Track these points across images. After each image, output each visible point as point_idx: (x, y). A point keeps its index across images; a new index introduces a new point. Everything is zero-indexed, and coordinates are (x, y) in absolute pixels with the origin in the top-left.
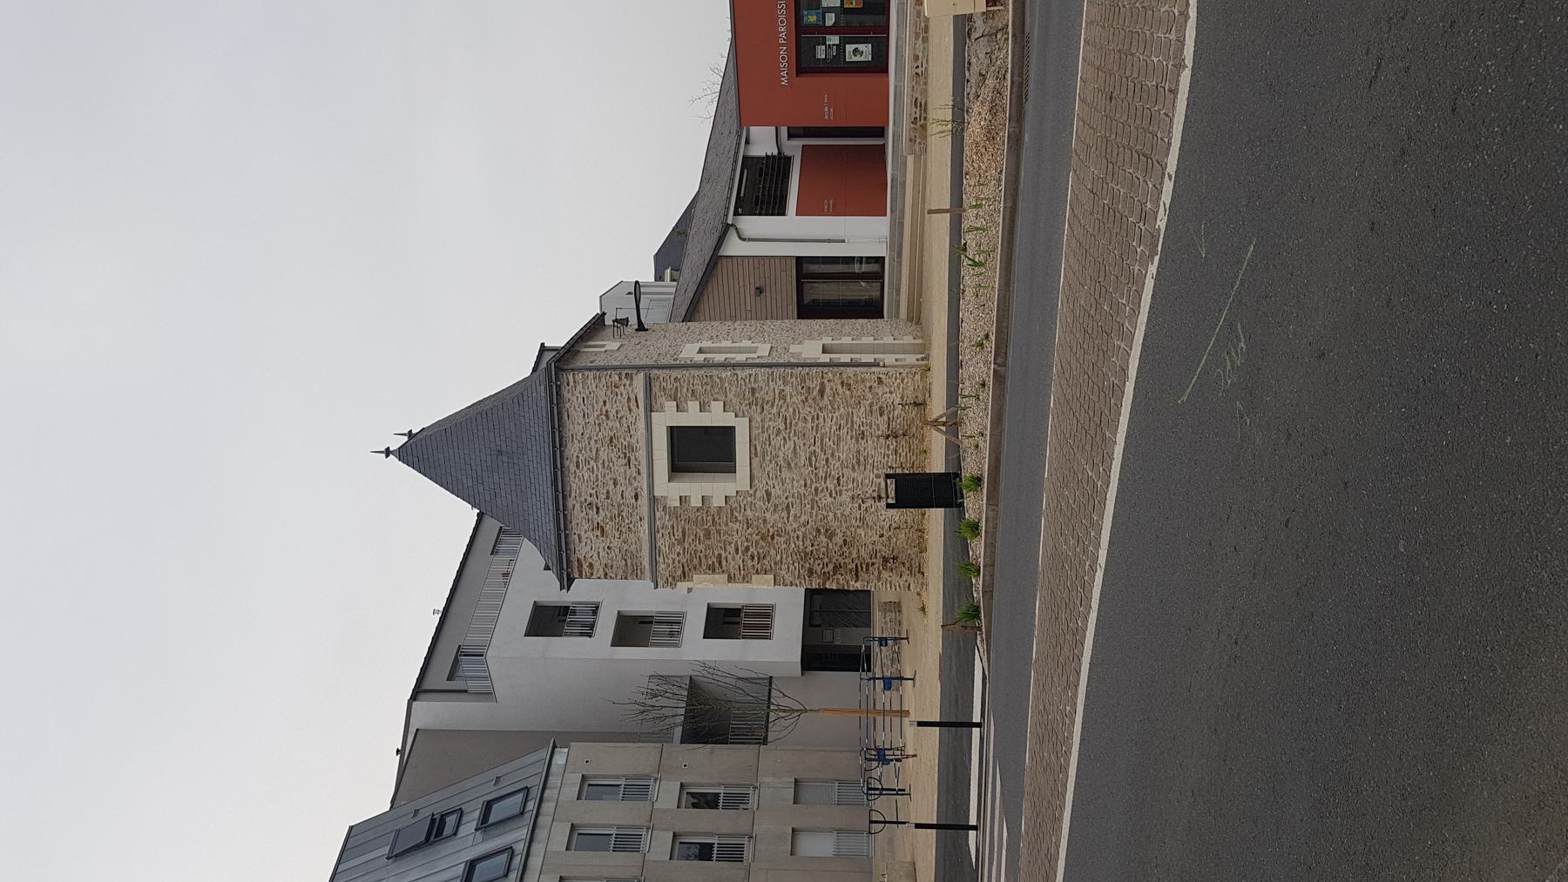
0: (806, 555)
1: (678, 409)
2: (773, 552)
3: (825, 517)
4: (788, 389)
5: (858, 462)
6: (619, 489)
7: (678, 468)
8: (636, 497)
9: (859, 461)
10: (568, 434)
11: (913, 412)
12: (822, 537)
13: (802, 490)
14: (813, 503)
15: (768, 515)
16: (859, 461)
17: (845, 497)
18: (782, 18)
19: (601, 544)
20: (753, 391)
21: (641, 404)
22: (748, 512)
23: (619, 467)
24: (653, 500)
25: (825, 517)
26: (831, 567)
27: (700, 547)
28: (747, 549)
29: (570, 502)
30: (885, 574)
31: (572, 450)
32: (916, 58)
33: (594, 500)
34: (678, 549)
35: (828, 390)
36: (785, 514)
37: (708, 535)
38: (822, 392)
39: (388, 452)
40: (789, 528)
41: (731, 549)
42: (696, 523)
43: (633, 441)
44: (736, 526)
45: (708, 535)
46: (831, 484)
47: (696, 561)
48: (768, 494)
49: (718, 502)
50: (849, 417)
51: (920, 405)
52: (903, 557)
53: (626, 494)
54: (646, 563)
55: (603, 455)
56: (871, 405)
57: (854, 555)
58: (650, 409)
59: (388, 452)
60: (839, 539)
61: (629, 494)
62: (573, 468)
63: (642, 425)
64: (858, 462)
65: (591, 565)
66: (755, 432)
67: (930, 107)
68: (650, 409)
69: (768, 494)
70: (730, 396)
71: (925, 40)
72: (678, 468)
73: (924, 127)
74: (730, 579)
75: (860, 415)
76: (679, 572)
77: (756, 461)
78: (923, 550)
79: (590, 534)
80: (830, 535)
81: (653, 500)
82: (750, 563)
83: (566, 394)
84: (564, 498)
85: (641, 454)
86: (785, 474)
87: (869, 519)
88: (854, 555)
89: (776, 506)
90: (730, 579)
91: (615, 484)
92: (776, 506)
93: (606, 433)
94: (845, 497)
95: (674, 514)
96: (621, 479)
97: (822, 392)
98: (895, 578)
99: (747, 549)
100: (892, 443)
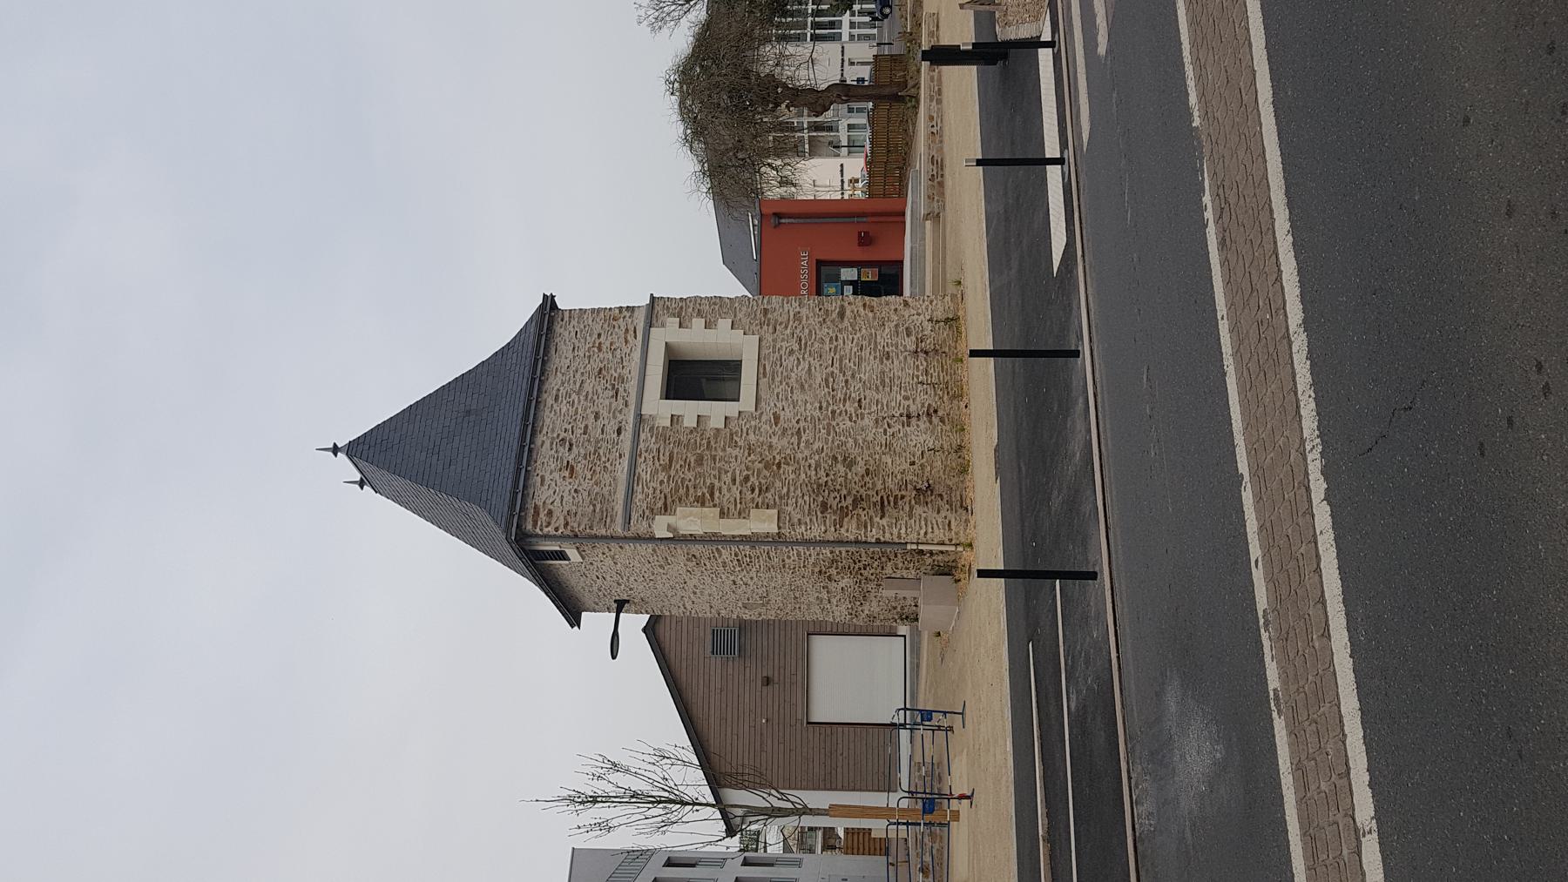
0: (819, 488)
1: (680, 326)
2: (778, 484)
3: (844, 444)
4: (804, 311)
5: (883, 382)
6: (600, 423)
7: (674, 389)
8: (619, 432)
9: (884, 382)
10: (551, 367)
11: (945, 333)
12: (840, 466)
13: (817, 413)
14: (828, 428)
15: (774, 440)
16: (884, 382)
17: (868, 421)
18: (804, 282)
19: (566, 487)
20: (766, 311)
21: (640, 337)
22: (752, 437)
23: (604, 401)
24: (640, 417)
25: (844, 444)
26: (850, 500)
27: (690, 475)
28: (747, 479)
29: (540, 439)
30: (918, 510)
31: (553, 383)
32: (931, 118)
33: (568, 436)
34: (662, 476)
35: (848, 313)
36: (795, 440)
37: (700, 460)
38: (842, 315)
39: (335, 450)
40: (800, 456)
41: (727, 478)
42: (687, 446)
43: (625, 372)
44: (736, 452)
45: (700, 460)
46: (851, 407)
47: (682, 492)
48: (777, 418)
49: (716, 422)
50: (872, 339)
51: (952, 321)
52: (939, 489)
53: (608, 429)
54: (619, 508)
55: (588, 387)
56: (897, 326)
57: (879, 486)
58: (650, 325)
59: (335, 450)
60: (860, 469)
61: (611, 427)
62: (550, 401)
63: (637, 355)
64: (883, 382)
65: (550, 513)
66: (765, 352)
67: (947, 162)
68: (650, 325)
69: (777, 418)
70: (740, 315)
71: (939, 102)
72: (674, 389)
73: (941, 184)
74: (722, 514)
75: (884, 337)
76: (660, 504)
77: (763, 381)
78: (964, 470)
79: (556, 475)
80: (850, 463)
81: (640, 417)
82: (749, 496)
83: (558, 329)
84: (533, 434)
85: (632, 387)
86: (798, 396)
87: (898, 445)
88: (879, 486)
89: (785, 430)
90: (722, 514)
91: (597, 417)
92: (785, 430)
93: (596, 365)
94: (868, 421)
95: (663, 436)
96: (604, 413)
97: (842, 315)
98: (932, 515)
99: (747, 479)
100: (922, 362)
